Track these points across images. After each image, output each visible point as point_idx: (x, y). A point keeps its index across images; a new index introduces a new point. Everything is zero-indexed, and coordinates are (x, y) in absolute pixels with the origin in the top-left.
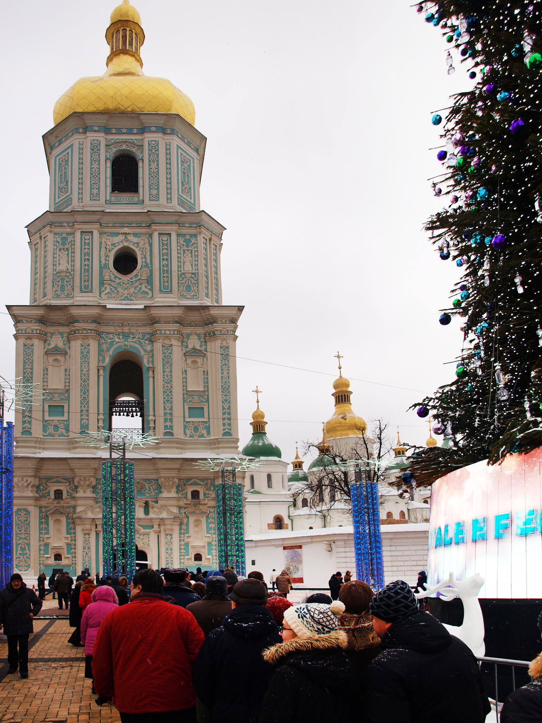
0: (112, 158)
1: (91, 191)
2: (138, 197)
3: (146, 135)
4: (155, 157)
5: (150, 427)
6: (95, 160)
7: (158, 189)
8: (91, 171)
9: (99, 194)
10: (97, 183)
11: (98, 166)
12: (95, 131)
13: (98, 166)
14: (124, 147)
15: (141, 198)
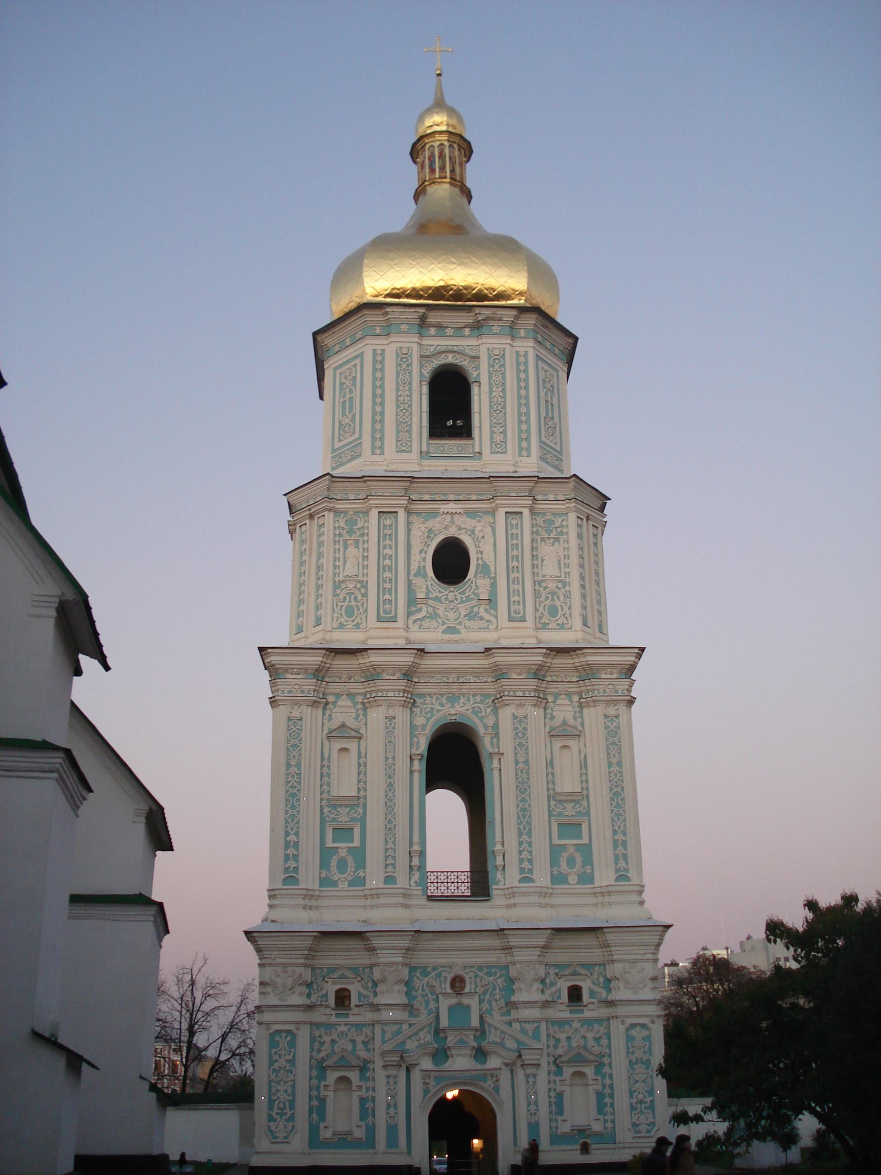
0: (428, 380)
1: (397, 437)
2: (473, 446)
3: (484, 340)
4: (500, 378)
5: (496, 867)
6: (403, 383)
7: (504, 432)
8: (397, 400)
9: (411, 441)
10: (407, 422)
11: (407, 393)
12: (404, 332)
13: (407, 393)
14: (450, 359)
15: (477, 450)
